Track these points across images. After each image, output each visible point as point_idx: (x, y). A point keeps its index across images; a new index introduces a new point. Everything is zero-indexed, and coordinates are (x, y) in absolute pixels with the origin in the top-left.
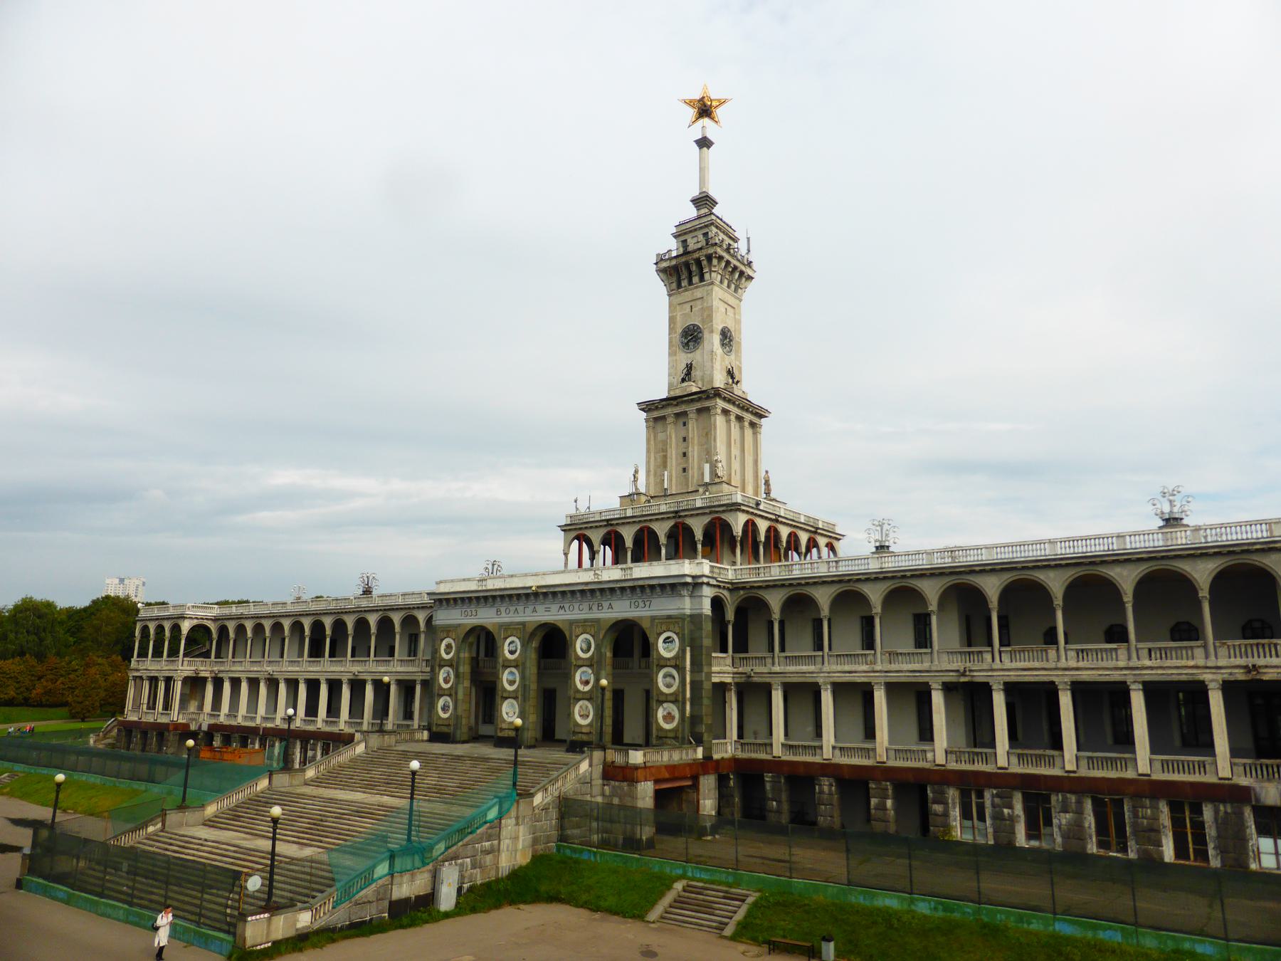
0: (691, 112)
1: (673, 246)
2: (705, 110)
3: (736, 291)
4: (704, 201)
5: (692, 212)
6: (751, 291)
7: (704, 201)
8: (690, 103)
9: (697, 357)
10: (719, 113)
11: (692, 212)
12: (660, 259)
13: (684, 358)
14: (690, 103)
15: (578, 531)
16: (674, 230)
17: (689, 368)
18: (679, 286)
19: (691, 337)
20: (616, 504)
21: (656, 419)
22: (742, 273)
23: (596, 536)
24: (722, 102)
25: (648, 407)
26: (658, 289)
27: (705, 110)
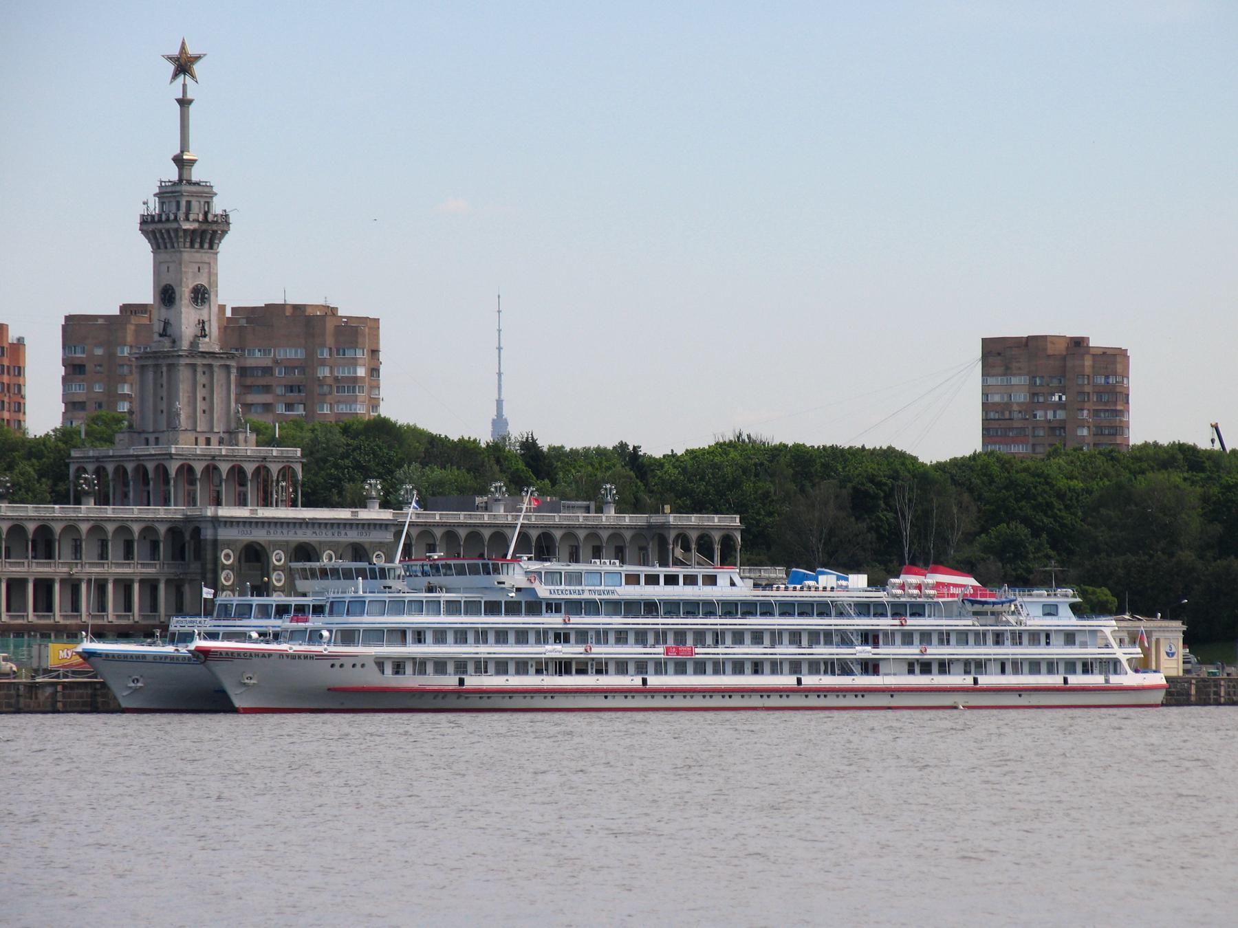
0: (171, 68)
1: (154, 207)
2: (183, 65)
3: (211, 247)
4: (181, 162)
5: (172, 174)
6: (226, 246)
8: (170, 58)
10: (197, 68)
11: (172, 174)
14: (170, 58)
16: (157, 191)
18: (159, 248)
21: (143, 366)
22: (215, 232)
24: (198, 58)
26: (143, 249)
27: (183, 65)
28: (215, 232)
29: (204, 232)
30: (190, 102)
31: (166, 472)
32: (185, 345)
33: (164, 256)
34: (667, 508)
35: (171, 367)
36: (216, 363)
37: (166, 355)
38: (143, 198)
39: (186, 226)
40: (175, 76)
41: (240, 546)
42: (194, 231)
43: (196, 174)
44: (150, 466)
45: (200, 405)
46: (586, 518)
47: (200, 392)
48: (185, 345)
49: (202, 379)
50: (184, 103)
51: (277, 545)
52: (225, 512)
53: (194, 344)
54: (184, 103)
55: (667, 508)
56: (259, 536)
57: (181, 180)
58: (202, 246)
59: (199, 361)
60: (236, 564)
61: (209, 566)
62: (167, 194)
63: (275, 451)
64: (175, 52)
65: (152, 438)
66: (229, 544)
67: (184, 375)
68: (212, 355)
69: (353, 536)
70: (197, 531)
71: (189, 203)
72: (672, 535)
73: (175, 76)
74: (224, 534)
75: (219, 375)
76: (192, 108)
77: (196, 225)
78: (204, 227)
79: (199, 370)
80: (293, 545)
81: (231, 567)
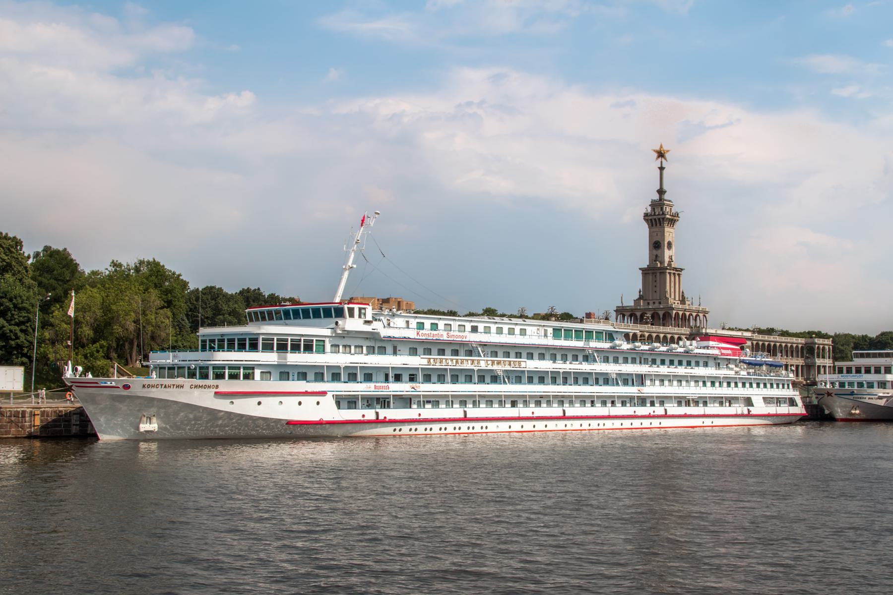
0: (656, 155)
4: (661, 192)
5: (656, 197)
7: (661, 192)
9: (658, 252)
11: (656, 197)
12: (646, 215)
13: (655, 252)
15: (622, 312)
17: (657, 256)
19: (656, 245)
20: (632, 304)
23: (627, 314)
26: (645, 227)
27: (661, 154)
33: (655, 229)
35: (664, 273)
37: (660, 268)
38: (645, 207)
39: (668, 216)
43: (666, 197)
45: (672, 290)
50: (661, 169)
53: (669, 264)
54: (661, 169)
57: (660, 199)
62: (654, 204)
64: (658, 148)
65: (651, 302)
67: (668, 276)
75: (677, 277)
76: (665, 171)
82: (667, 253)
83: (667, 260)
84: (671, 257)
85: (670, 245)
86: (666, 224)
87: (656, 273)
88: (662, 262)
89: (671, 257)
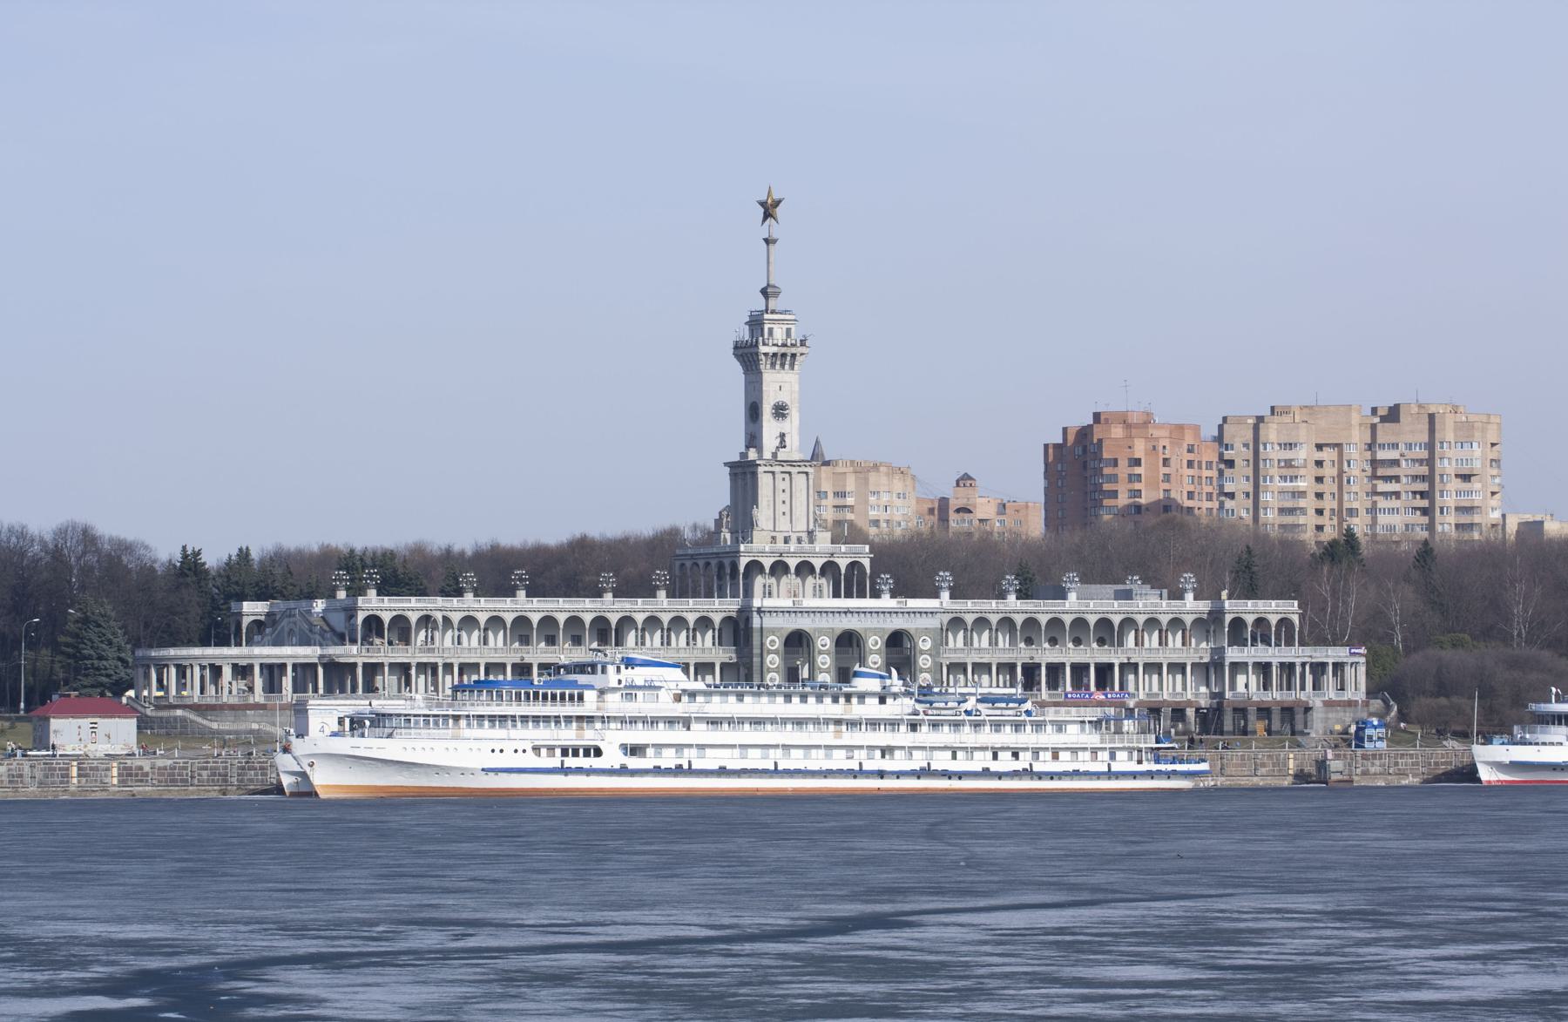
2: (769, 210)
5: (760, 303)
10: (779, 211)
11: (760, 303)
19: (754, 412)
25: (732, 465)
27: (769, 210)
28: (793, 356)
29: (784, 355)
30: (775, 241)
31: (735, 566)
32: (767, 455)
34: (1224, 594)
35: (754, 475)
36: (794, 470)
39: (763, 349)
40: (765, 220)
41: (785, 634)
42: (775, 355)
44: (727, 562)
46: (1145, 605)
47: (781, 497)
48: (767, 455)
49: (781, 485)
51: (822, 632)
52: (769, 603)
53: (775, 455)
55: (1224, 594)
56: (804, 623)
58: (783, 365)
59: (777, 469)
60: (782, 648)
61: (756, 651)
63: (843, 548)
66: (773, 631)
67: (764, 481)
68: (791, 463)
69: (898, 623)
70: (748, 620)
71: (771, 330)
72: (1228, 618)
73: (765, 220)
74: (769, 622)
77: (775, 349)
78: (783, 350)
79: (779, 477)
80: (838, 633)
81: (776, 652)
82: (770, 429)
83: (769, 441)
84: (782, 436)
85: (780, 411)
86: (764, 365)
87: (743, 475)
88: (760, 450)
89: (782, 436)
